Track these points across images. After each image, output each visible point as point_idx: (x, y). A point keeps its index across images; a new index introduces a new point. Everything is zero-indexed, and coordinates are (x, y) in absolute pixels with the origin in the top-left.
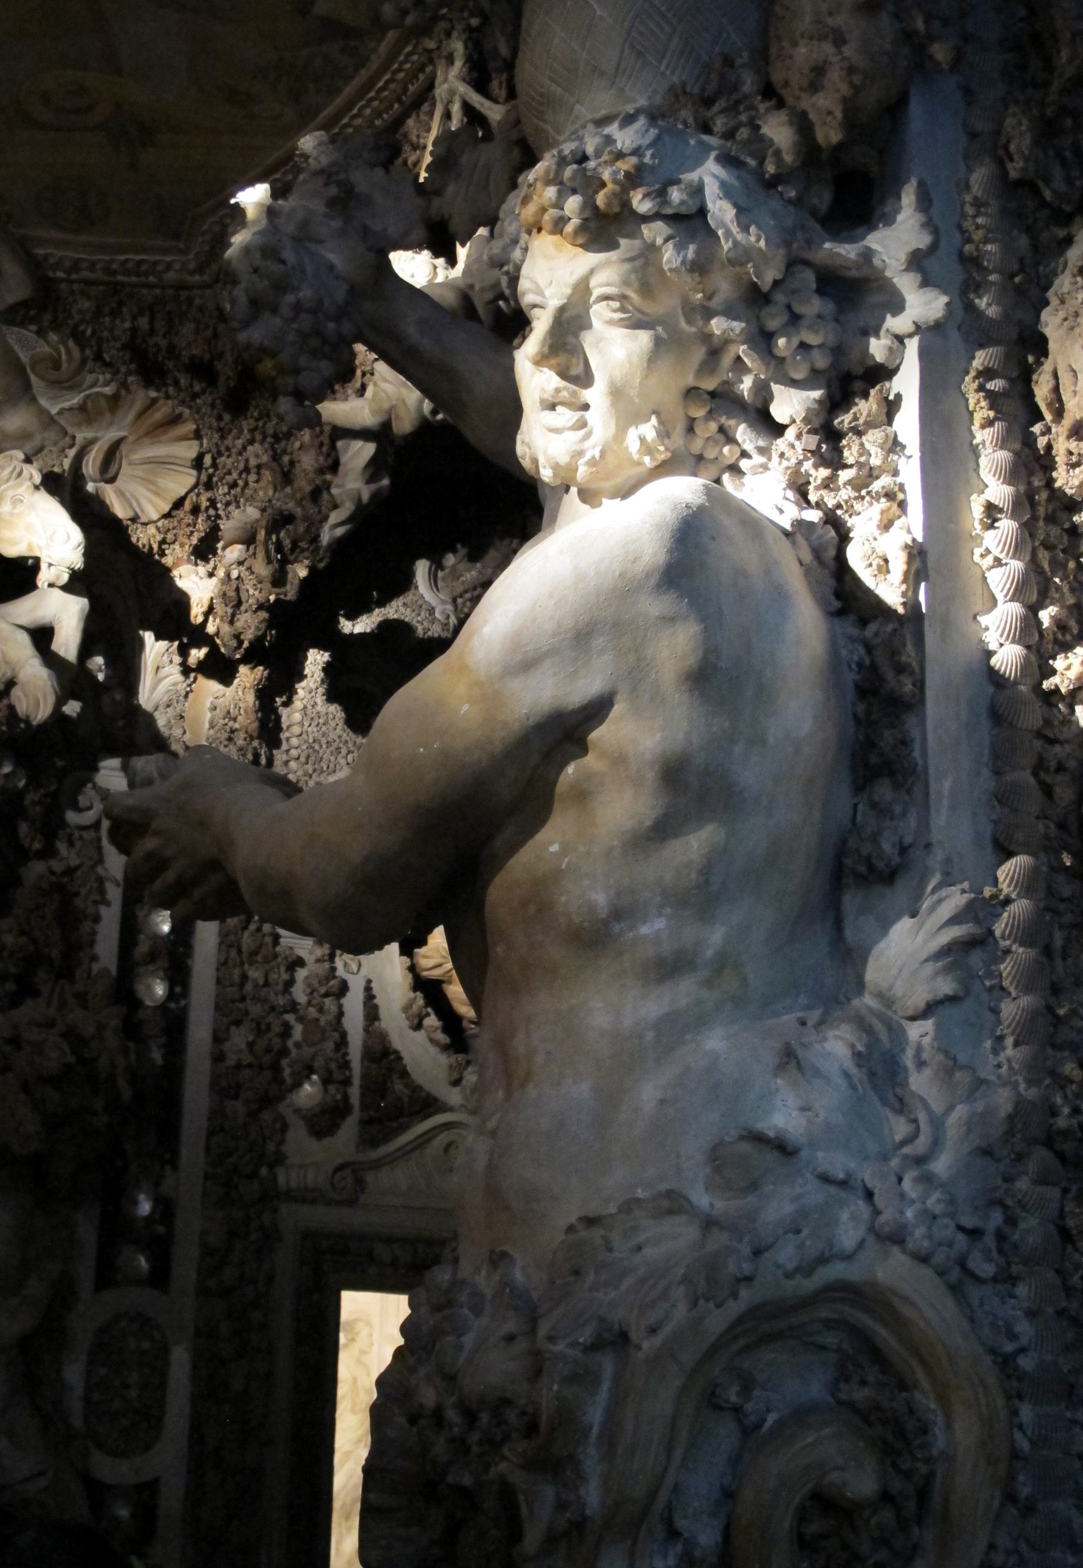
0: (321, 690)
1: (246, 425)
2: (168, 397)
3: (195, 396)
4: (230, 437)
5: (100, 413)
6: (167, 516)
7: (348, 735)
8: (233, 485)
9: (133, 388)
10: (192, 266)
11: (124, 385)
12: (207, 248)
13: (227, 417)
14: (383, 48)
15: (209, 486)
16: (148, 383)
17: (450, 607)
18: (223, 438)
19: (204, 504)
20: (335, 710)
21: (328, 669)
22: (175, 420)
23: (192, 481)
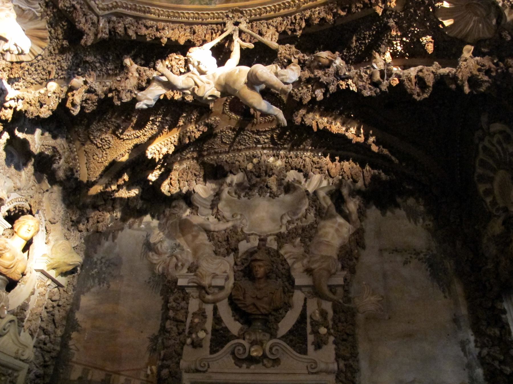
0: (3, 146)
1: (58, 58)
2: (50, 32)
3: (57, 38)
4: (50, 57)
5: (25, 17)
6: (12, 63)
7: (4, 163)
8: (36, 70)
9: (44, 20)
10: (100, 6)
11: (42, 17)
12: (110, 6)
13: (57, 52)
14: (219, 6)
15: (31, 65)
16: (50, 24)
17: (39, 147)
18: (49, 56)
19: (26, 69)
20: (4, 153)
21: (8, 140)
22: (43, 39)
23: (30, 59)
